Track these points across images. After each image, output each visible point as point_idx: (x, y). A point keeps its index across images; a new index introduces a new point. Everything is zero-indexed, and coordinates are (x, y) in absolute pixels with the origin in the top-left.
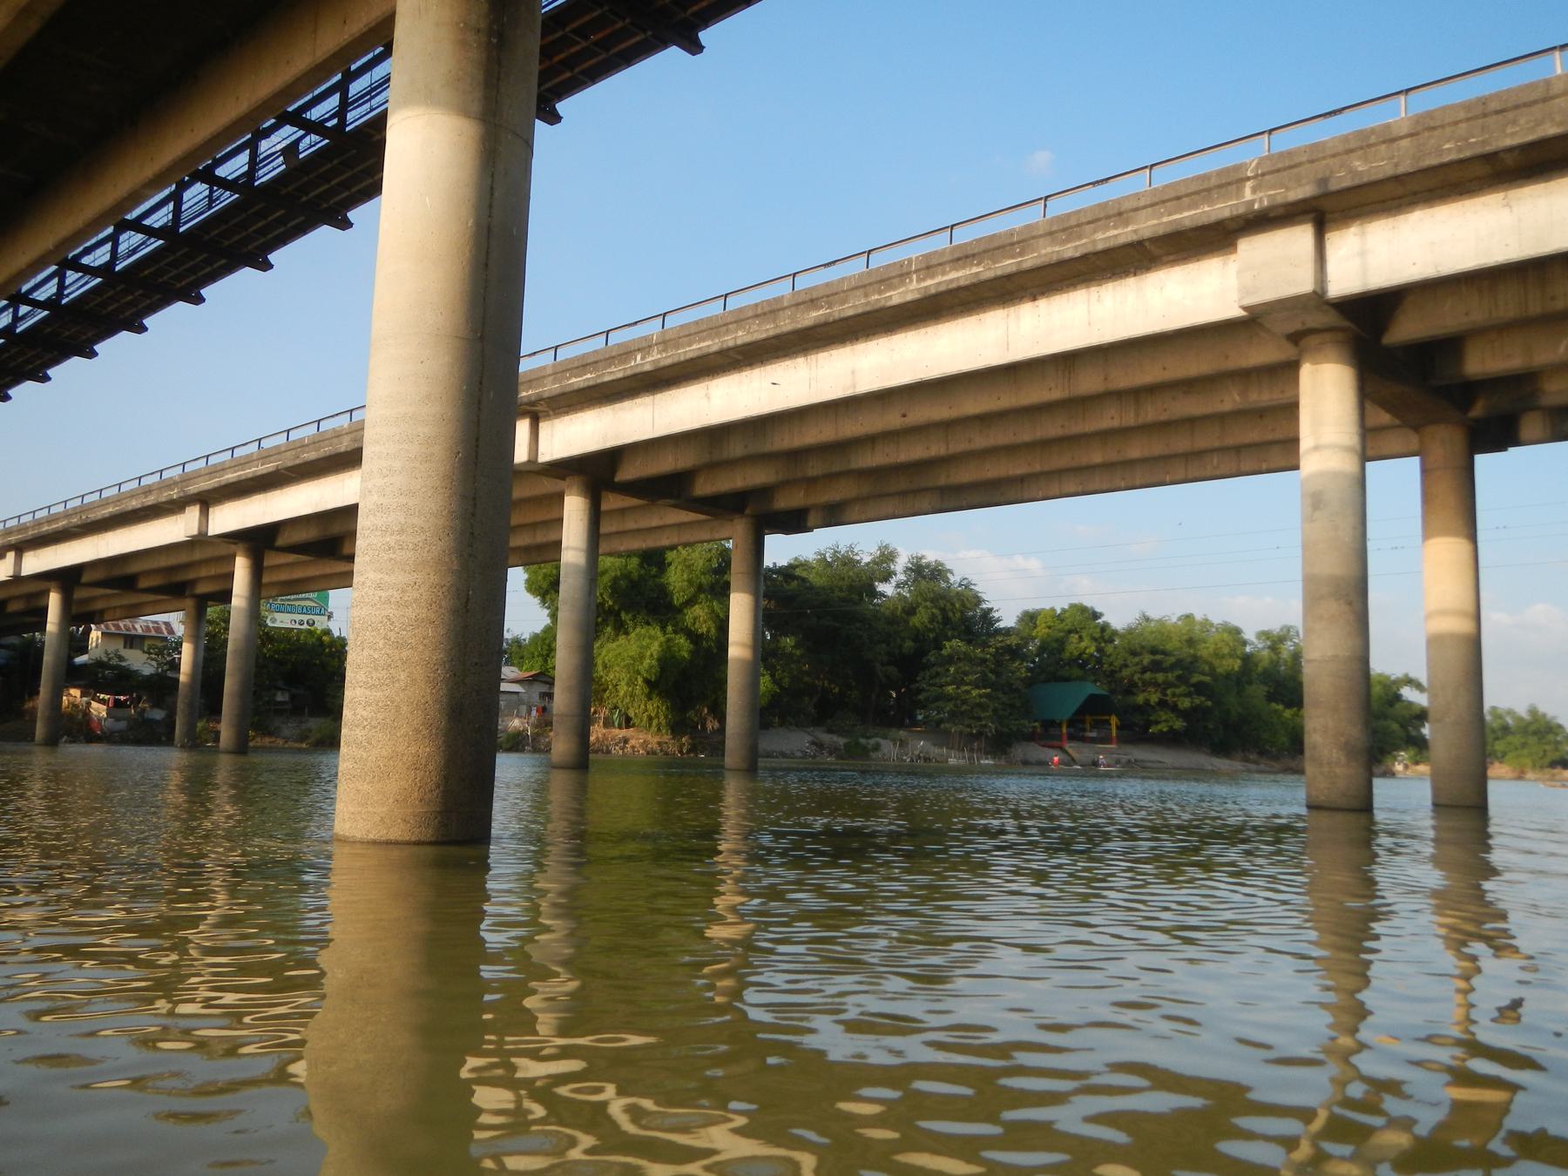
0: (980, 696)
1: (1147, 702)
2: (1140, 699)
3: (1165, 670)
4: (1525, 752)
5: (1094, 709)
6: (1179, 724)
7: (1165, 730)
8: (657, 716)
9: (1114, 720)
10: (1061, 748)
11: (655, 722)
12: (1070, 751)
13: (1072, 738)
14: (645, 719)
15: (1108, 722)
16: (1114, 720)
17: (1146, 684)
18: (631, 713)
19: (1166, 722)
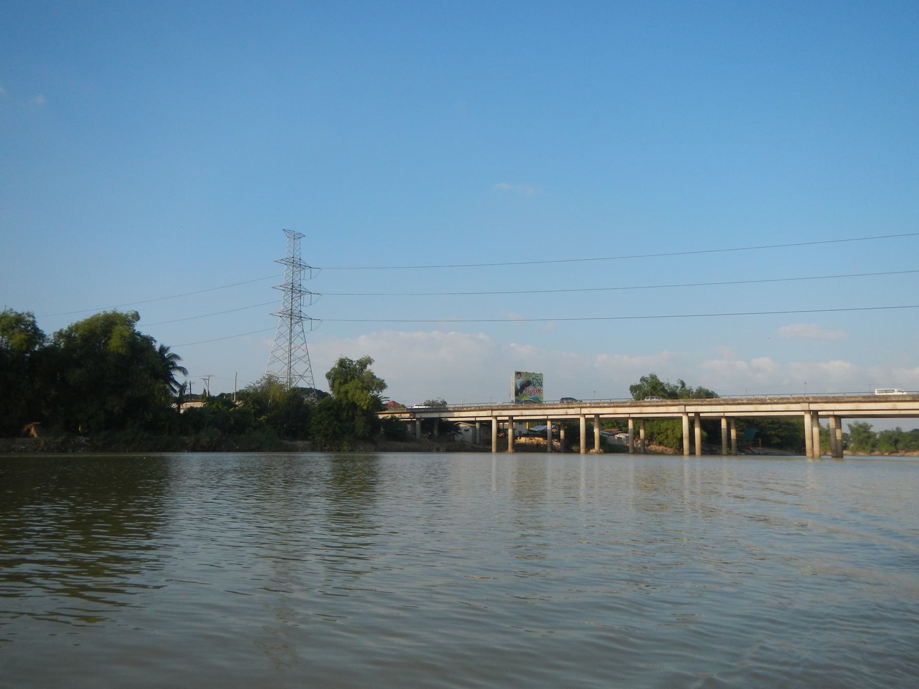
0: (743, 435)
1: (771, 434)
2: (769, 433)
3: (775, 424)
4: (827, 443)
5: (757, 435)
6: (779, 441)
7: (776, 442)
8: (676, 443)
9: (760, 440)
10: (749, 449)
11: (675, 445)
12: (753, 450)
13: (753, 445)
14: (672, 444)
15: (758, 441)
16: (760, 440)
17: (769, 428)
18: (665, 442)
19: (776, 440)
